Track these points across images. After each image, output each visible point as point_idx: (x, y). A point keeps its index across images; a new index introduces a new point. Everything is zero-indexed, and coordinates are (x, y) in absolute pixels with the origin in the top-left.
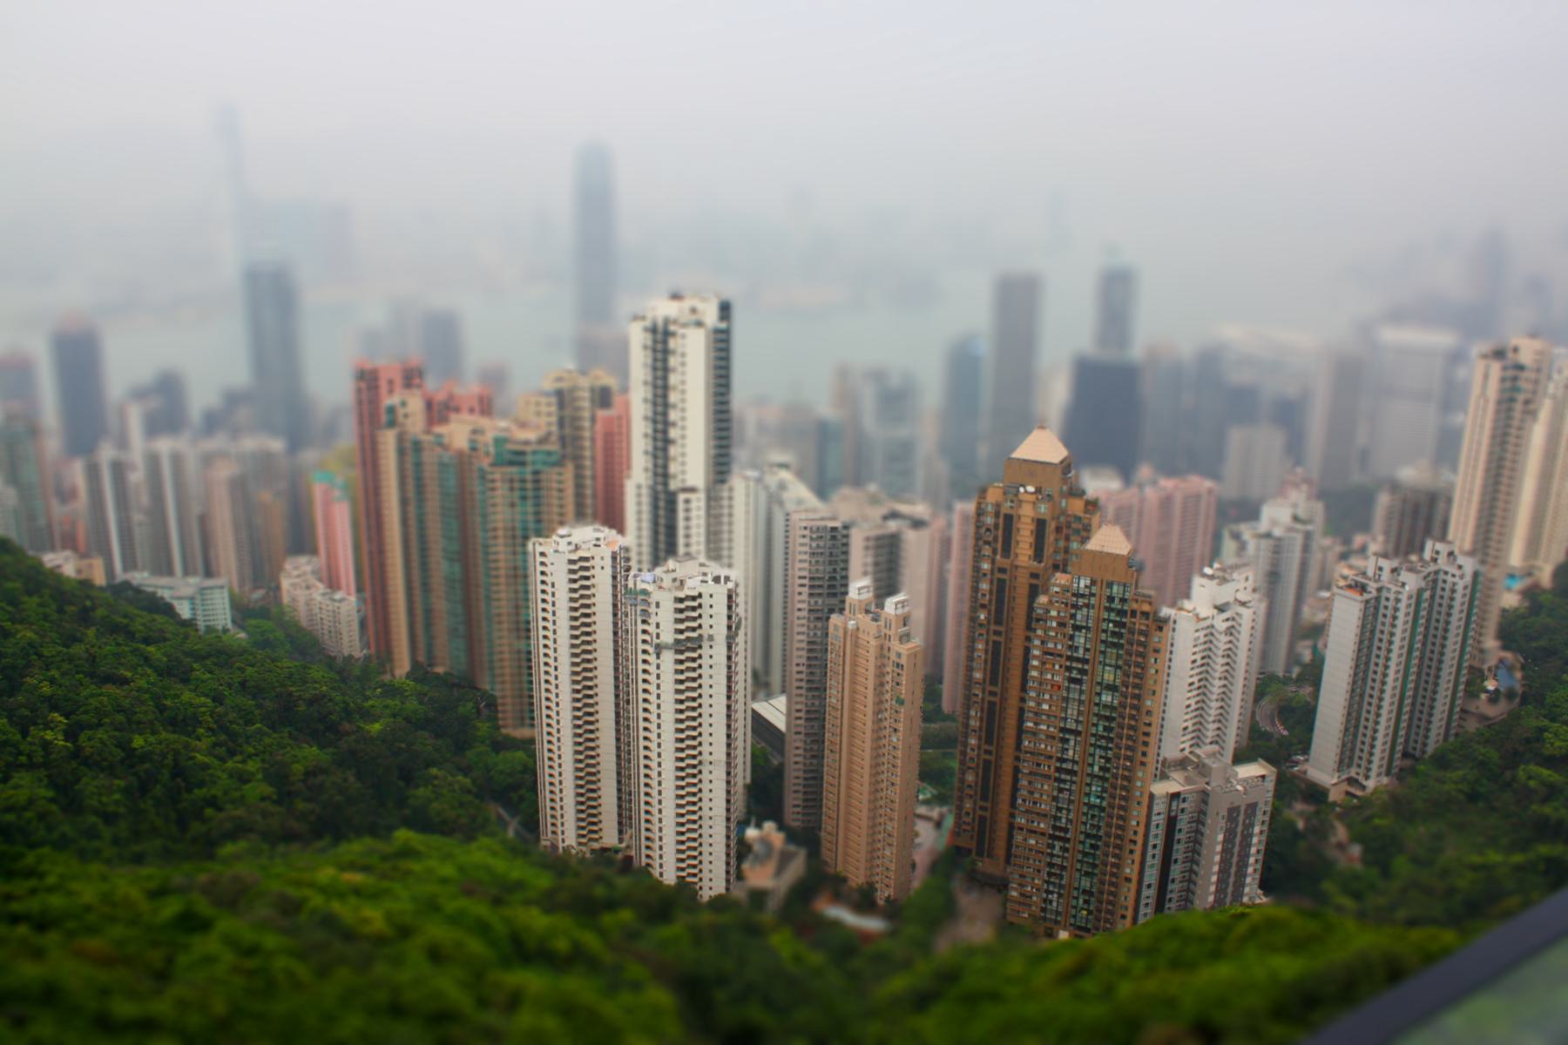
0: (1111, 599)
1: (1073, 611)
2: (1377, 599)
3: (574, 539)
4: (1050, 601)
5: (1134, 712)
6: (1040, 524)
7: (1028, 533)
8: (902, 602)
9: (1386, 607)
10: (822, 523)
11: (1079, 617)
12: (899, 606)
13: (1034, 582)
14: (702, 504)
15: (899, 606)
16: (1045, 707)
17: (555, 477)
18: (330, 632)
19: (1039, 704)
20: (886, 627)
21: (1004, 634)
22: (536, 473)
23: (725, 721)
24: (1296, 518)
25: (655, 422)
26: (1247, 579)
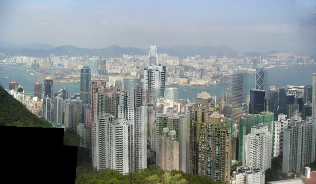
0: (216, 129)
1: (208, 132)
11: (209, 133)
24: (286, 118)
26: (266, 129)
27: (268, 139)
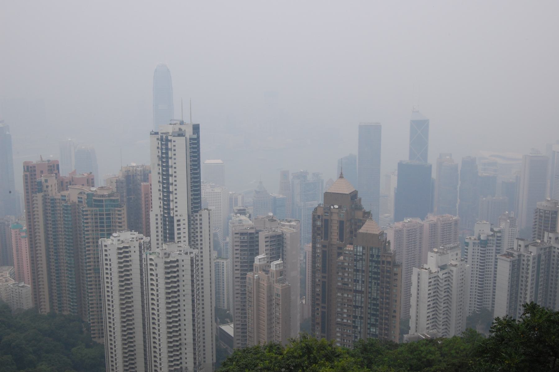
0: (372, 256)
1: (355, 262)
2: (519, 260)
3: (122, 238)
4: (344, 259)
5: (387, 311)
6: (341, 223)
7: (336, 228)
8: (279, 264)
9: (523, 265)
10: (245, 231)
11: (358, 265)
12: (278, 266)
13: (340, 251)
14: (186, 222)
15: (278, 266)
16: (345, 311)
17: (117, 212)
18: (17, 303)
19: (342, 309)
20: (272, 277)
21: (327, 278)
22: (109, 210)
23: (191, 323)
25: (163, 183)
26: (457, 254)
27: (462, 277)
